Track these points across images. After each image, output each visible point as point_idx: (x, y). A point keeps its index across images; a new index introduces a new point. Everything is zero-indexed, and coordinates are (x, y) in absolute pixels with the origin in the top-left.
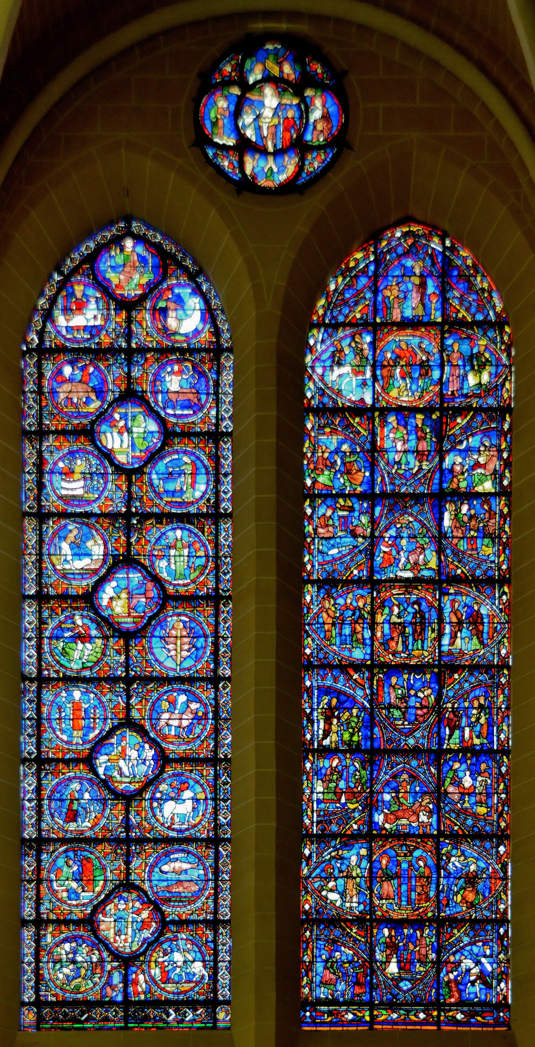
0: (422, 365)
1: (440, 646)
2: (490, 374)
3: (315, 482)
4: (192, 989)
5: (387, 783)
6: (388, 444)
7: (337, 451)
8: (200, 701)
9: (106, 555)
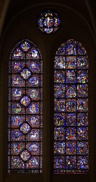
0: (73, 62)
1: (77, 109)
2: (84, 64)
3: (56, 81)
5: (68, 132)
6: (68, 75)
7: (60, 76)
8: (37, 118)
9: (22, 94)
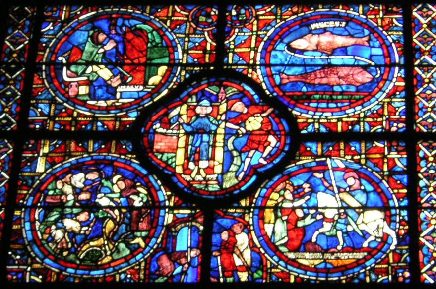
4: (359, 263)
